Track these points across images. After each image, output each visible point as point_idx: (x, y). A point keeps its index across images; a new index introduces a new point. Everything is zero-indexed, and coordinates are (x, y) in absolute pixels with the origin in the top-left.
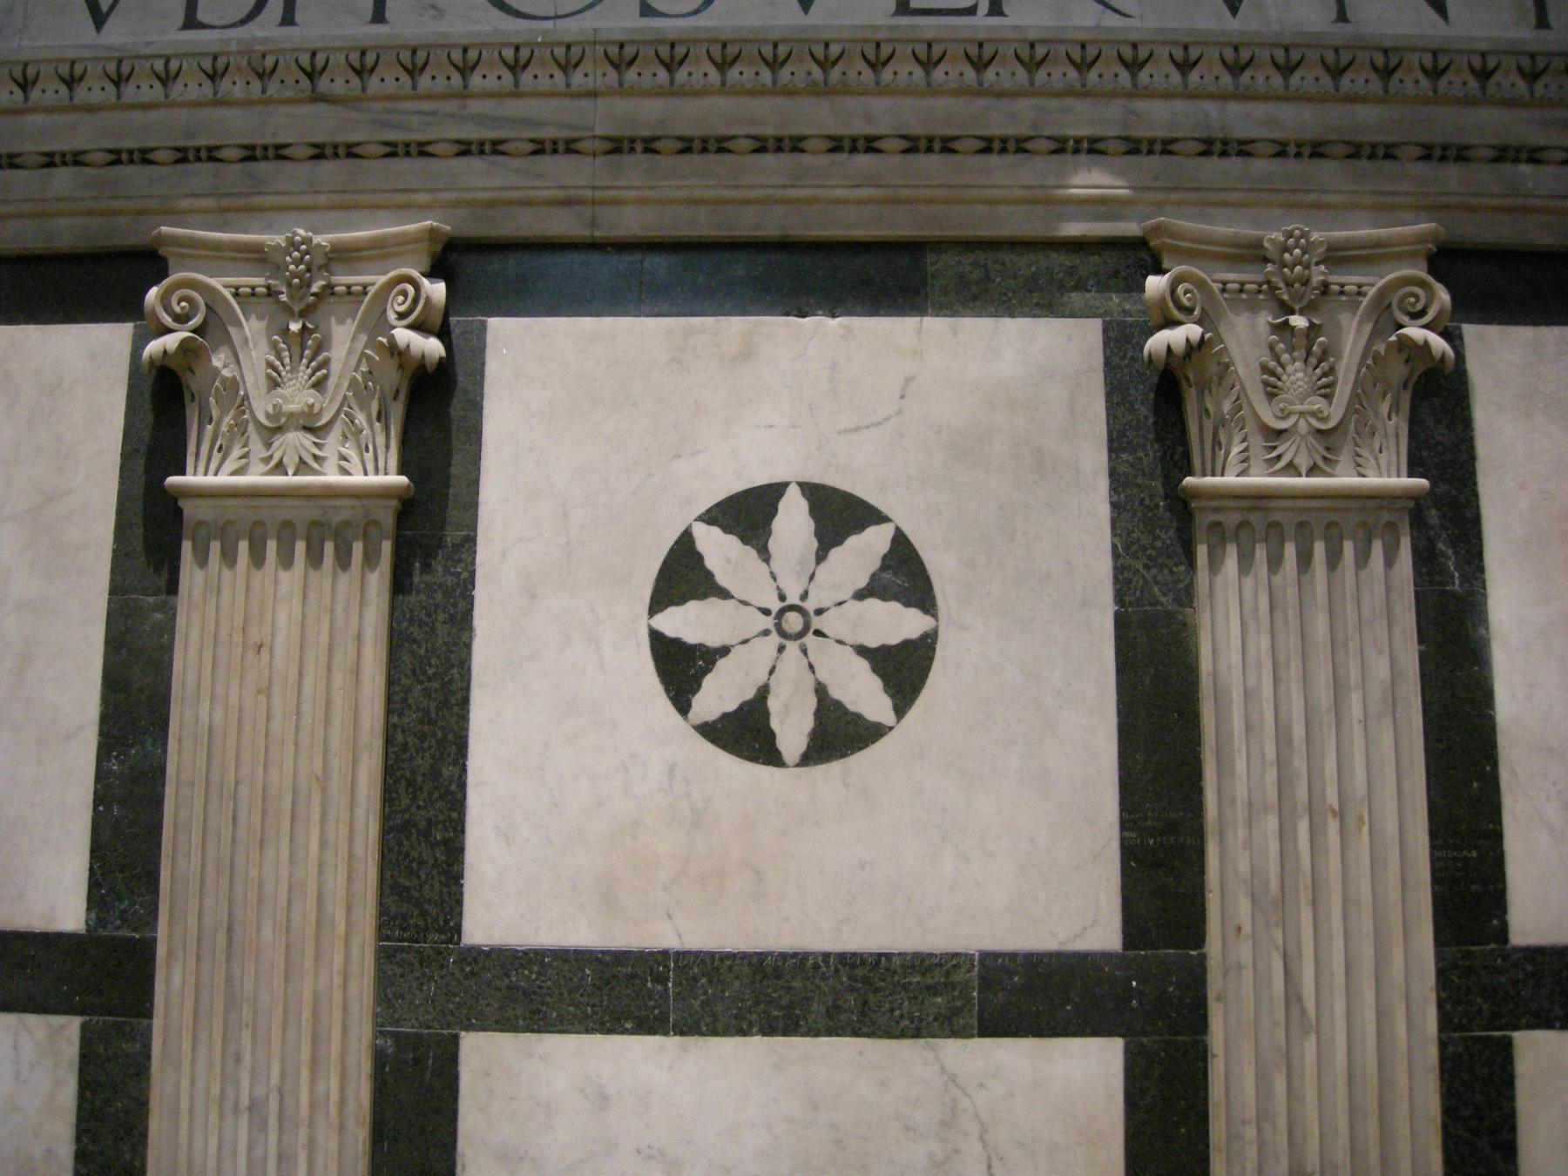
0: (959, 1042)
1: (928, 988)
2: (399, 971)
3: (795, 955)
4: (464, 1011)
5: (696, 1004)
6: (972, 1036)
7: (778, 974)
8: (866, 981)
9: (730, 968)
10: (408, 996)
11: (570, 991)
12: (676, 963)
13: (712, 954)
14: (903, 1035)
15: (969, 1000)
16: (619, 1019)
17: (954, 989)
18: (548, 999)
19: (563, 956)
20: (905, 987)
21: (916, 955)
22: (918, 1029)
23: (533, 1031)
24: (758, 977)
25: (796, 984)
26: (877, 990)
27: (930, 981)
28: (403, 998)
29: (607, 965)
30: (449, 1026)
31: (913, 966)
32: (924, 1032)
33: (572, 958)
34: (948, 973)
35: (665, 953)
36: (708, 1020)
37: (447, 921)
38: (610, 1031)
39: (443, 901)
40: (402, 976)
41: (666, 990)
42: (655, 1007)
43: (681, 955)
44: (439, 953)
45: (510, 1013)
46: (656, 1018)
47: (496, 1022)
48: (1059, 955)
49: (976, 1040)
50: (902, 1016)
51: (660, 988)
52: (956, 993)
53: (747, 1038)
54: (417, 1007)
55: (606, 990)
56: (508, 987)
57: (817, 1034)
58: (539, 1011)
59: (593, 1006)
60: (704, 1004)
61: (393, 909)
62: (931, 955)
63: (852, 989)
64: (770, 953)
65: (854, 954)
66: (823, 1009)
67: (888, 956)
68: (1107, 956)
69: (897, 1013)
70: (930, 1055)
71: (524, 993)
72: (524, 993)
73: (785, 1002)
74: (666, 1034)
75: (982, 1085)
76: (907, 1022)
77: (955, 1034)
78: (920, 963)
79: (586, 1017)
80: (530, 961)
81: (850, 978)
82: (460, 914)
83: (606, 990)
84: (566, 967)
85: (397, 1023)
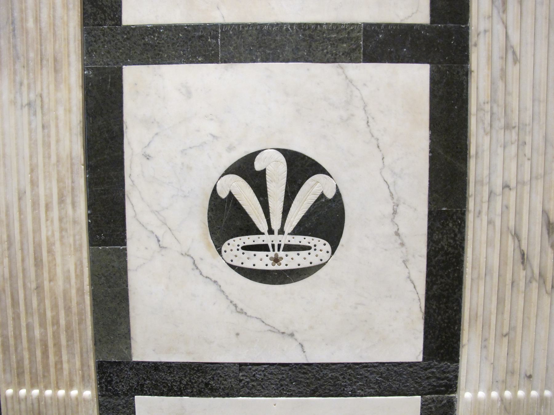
0: (354, 65)
1: (340, 40)
2: (93, 39)
3: (278, 24)
4: (125, 56)
5: (232, 48)
6: (360, 62)
7: (269, 33)
8: (311, 36)
9: (247, 31)
10: (98, 51)
11: (173, 44)
12: (222, 29)
13: (238, 25)
14: (328, 62)
15: (359, 46)
16: (195, 57)
17: (352, 40)
18: (163, 49)
20: (329, 39)
21: (334, 24)
22: (335, 59)
23: (156, 64)
24: (260, 35)
25: (278, 38)
26: (316, 41)
27: (341, 37)
28: (96, 52)
29: (189, 32)
30: (117, 63)
31: (333, 30)
32: (338, 60)
33: (173, 30)
34: (349, 33)
35: (216, 25)
36: (237, 55)
37: (114, 15)
39: (112, 6)
40: (95, 41)
41: (217, 42)
42: (212, 50)
43: (223, 26)
44: (111, 30)
45: (145, 56)
47: (139, 60)
48: (401, 25)
49: (362, 64)
50: (327, 53)
51: (214, 41)
52: (353, 42)
53: (256, 63)
54: (103, 55)
55: (189, 43)
56: (144, 44)
57: (287, 61)
58: (159, 54)
59: (183, 51)
60: (235, 48)
61: (90, 11)
62: (341, 24)
63: (304, 40)
64: (266, 24)
65: (305, 24)
66: (290, 50)
67: (321, 25)
68: (422, 26)
69: (325, 51)
70: (340, 71)
71: (152, 46)
72: (152, 46)
73: (273, 46)
74: (217, 63)
75: (365, 85)
76: (330, 56)
77: (352, 61)
78: (336, 28)
79: (181, 56)
80: (154, 32)
81: (303, 35)
82: (121, 11)
83: (189, 43)
84: (170, 34)
85: (94, 63)
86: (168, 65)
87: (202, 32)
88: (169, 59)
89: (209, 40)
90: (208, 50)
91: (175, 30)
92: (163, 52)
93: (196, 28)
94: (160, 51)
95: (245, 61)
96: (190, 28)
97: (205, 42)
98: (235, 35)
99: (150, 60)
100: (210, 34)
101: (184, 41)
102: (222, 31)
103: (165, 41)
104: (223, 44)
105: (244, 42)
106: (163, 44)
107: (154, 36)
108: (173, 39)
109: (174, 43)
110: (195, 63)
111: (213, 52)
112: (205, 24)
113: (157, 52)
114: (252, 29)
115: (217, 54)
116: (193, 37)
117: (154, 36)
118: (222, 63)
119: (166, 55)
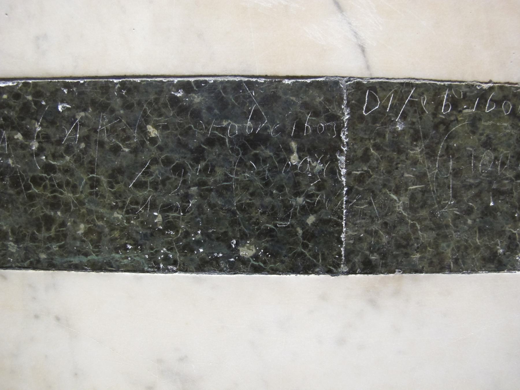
5: (400, 203)
9: (474, 120)
11: (115, 175)
13: (434, 90)
16: (225, 239)
18: (68, 195)
19: (97, 94)
23: (36, 265)
29: (196, 115)
33: (117, 103)
35: (328, 87)
36: (425, 237)
38: (204, 266)
41: (333, 172)
42: (306, 210)
46: (309, 236)
51: (319, 166)
53: (505, 275)
58: (49, 221)
59: (166, 209)
60: (416, 203)
72: (15, 183)
74: (332, 270)
79: (153, 233)
84: (104, 122)
86: (93, 275)
87: (257, 117)
88: (96, 244)
89: (294, 159)
90: (287, 207)
91: (128, 106)
92: (67, 209)
93: (231, 98)
94: (55, 205)
95: (460, 265)
96: (197, 99)
97: (275, 171)
98: (416, 138)
99: (12, 247)
100: (300, 127)
101: (167, 162)
102: (356, 118)
103: (78, 160)
104: (360, 179)
105: (456, 173)
106: (66, 171)
107: (28, 135)
108: (116, 150)
109: (120, 171)
110: (221, 271)
111: (311, 219)
112: (275, 81)
113: (40, 210)
114: (497, 114)
116: (211, 142)
117: (28, 135)
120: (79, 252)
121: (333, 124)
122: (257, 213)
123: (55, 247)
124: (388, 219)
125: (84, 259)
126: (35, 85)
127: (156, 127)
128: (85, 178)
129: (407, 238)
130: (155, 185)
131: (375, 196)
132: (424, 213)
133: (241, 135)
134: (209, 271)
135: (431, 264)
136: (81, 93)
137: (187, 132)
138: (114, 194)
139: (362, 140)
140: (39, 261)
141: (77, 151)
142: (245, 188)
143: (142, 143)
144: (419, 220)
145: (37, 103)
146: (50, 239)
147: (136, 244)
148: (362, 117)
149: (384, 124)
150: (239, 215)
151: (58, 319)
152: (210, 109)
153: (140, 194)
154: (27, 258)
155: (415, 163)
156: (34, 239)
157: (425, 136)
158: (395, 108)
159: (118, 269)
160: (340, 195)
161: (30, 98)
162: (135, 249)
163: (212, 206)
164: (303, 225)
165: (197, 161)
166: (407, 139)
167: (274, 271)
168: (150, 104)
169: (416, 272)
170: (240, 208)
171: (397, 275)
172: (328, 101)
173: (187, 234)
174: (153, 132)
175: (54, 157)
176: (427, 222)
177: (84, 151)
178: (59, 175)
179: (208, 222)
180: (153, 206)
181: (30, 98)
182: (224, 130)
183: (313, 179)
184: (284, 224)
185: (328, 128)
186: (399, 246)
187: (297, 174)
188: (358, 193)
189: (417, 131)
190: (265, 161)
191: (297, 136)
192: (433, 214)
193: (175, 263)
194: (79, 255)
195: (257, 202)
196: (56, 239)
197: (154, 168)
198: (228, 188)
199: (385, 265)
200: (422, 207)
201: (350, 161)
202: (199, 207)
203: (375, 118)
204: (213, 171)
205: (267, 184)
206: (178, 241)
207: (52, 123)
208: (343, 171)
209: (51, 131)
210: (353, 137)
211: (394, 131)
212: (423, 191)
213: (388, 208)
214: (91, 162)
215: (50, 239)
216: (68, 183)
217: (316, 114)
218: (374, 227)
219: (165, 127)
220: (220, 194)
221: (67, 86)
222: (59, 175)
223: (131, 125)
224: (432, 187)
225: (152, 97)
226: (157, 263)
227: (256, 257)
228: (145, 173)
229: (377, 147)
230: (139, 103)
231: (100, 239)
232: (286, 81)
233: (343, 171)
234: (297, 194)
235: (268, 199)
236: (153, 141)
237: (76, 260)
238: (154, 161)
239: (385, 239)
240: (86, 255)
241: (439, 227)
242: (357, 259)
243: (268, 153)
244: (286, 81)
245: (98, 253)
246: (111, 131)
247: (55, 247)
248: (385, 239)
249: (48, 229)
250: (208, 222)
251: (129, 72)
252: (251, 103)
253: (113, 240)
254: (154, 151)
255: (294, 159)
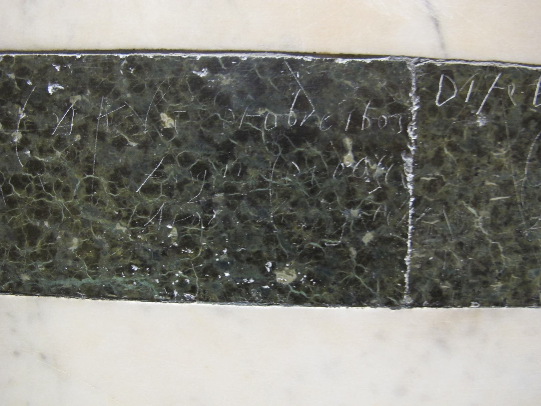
5: (479, 218)
11: (118, 176)
12: (426, 96)
16: (257, 260)
18: (58, 201)
29: (224, 101)
33: (123, 84)
35: (393, 69)
36: (510, 261)
38: (230, 294)
41: (397, 177)
42: (362, 225)
43: (435, 74)
46: (365, 258)
51: (379, 170)
58: (34, 233)
59: (184, 220)
60: (500, 219)
79: (165, 252)
83: (219, 176)
84: (106, 108)
87: (302, 105)
88: (93, 264)
89: (348, 160)
90: (338, 221)
91: (137, 89)
93: (269, 80)
94: (41, 212)
96: (225, 80)
98: (500, 136)
100: (357, 119)
101: (186, 160)
102: (428, 110)
103: (72, 156)
104: (431, 187)
106: (57, 169)
108: (120, 144)
109: (124, 171)
110: (252, 301)
111: (368, 237)
113: (22, 219)
115: (387, 254)
116: (243, 135)
118: (418, 303)
119: (75, 243)
120: (71, 274)
121: (399, 117)
122: (299, 228)
123: (40, 267)
124: (463, 238)
125: (78, 283)
126: (19, 59)
127: (172, 115)
128: (80, 180)
129: (486, 262)
130: (169, 190)
131: (448, 210)
132: (508, 231)
133: (281, 128)
134: (237, 301)
135: (515, 295)
136: (78, 71)
137: (211, 123)
138: (117, 200)
139: (434, 137)
140: (20, 284)
141: (70, 144)
142: (286, 195)
143: (154, 136)
144: (502, 240)
145: (21, 83)
146: (34, 256)
147: (143, 265)
148: (434, 109)
149: (461, 118)
150: (277, 231)
151: (43, 357)
152: (241, 94)
153: (150, 201)
154: (5, 280)
155: (499, 168)
156: (14, 255)
157: (513, 135)
158: (476, 99)
159: (119, 297)
160: (405, 208)
161: (12, 76)
162: (143, 271)
163: (243, 218)
164: (358, 244)
165: (224, 159)
166: (489, 137)
167: (320, 302)
168: (165, 86)
169: (497, 304)
170: (278, 221)
171: (474, 309)
172: (393, 87)
173: (209, 254)
174: (168, 121)
175: (42, 151)
176: (512, 243)
177: (80, 145)
178: (47, 175)
179: (237, 239)
180: (167, 217)
181: (12, 76)
182: (259, 121)
183: (371, 186)
184: (334, 243)
185: (392, 122)
186: (476, 273)
187: (352, 179)
188: (428, 204)
189: (502, 128)
190: (311, 162)
191: (353, 131)
192: (519, 233)
193: (193, 290)
194: (70, 277)
195: (299, 213)
196: (43, 256)
197: (168, 168)
198: (263, 196)
199: (459, 296)
200: (506, 224)
201: (419, 165)
202: (225, 219)
203: (450, 110)
204: (244, 173)
205: (313, 192)
206: (197, 262)
207: (40, 108)
208: (410, 177)
209: (38, 119)
210: (423, 134)
211: (475, 127)
212: (509, 204)
213: (464, 224)
214: (88, 159)
215: (34, 256)
216: (58, 186)
217: (377, 103)
218: (447, 249)
219: (184, 116)
220: (253, 204)
221: (60, 61)
222: (47, 175)
223: (141, 113)
224: (519, 199)
225: (168, 77)
226: (170, 290)
227: (297, 284)
228: (157, 175)
229: (453, 147)
230: (151, 85)
231: (97, 258)
232: (340, 61)
233: (410, 177)
234: (351, 205)
235: (314, 211)
236: (168, 133)
237: (67, 284)
238: (169, 159)
239: (459, 263)
240: (80, 277)
241: (526, 249)
242: (424, 289)
243: (315, 151)
244: (340, 61)
245: (95, 276)
246: (115, 120)
247: (40, 267)
248: (459, 263)
249: (33, 244)
250: (237, 239)
251: (138, 45)
252: (295, 87)
253: (113, 259)
254: (169, 147)
255: (348, 160)
